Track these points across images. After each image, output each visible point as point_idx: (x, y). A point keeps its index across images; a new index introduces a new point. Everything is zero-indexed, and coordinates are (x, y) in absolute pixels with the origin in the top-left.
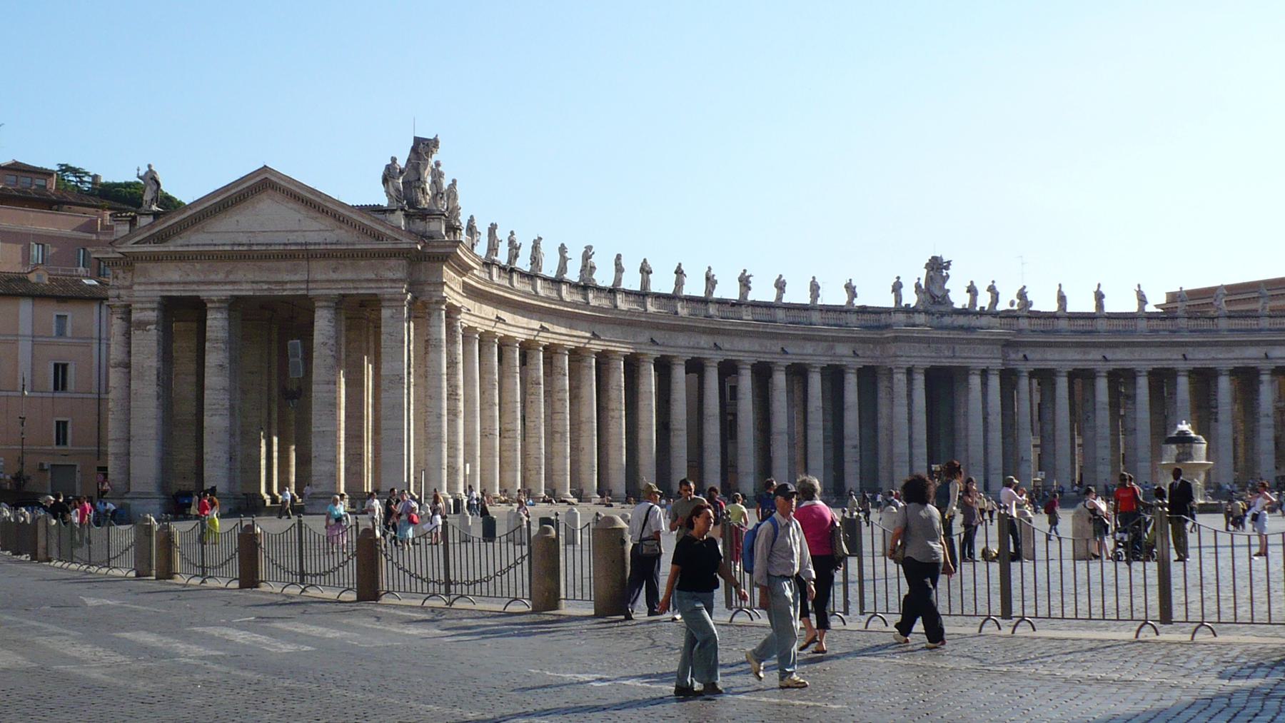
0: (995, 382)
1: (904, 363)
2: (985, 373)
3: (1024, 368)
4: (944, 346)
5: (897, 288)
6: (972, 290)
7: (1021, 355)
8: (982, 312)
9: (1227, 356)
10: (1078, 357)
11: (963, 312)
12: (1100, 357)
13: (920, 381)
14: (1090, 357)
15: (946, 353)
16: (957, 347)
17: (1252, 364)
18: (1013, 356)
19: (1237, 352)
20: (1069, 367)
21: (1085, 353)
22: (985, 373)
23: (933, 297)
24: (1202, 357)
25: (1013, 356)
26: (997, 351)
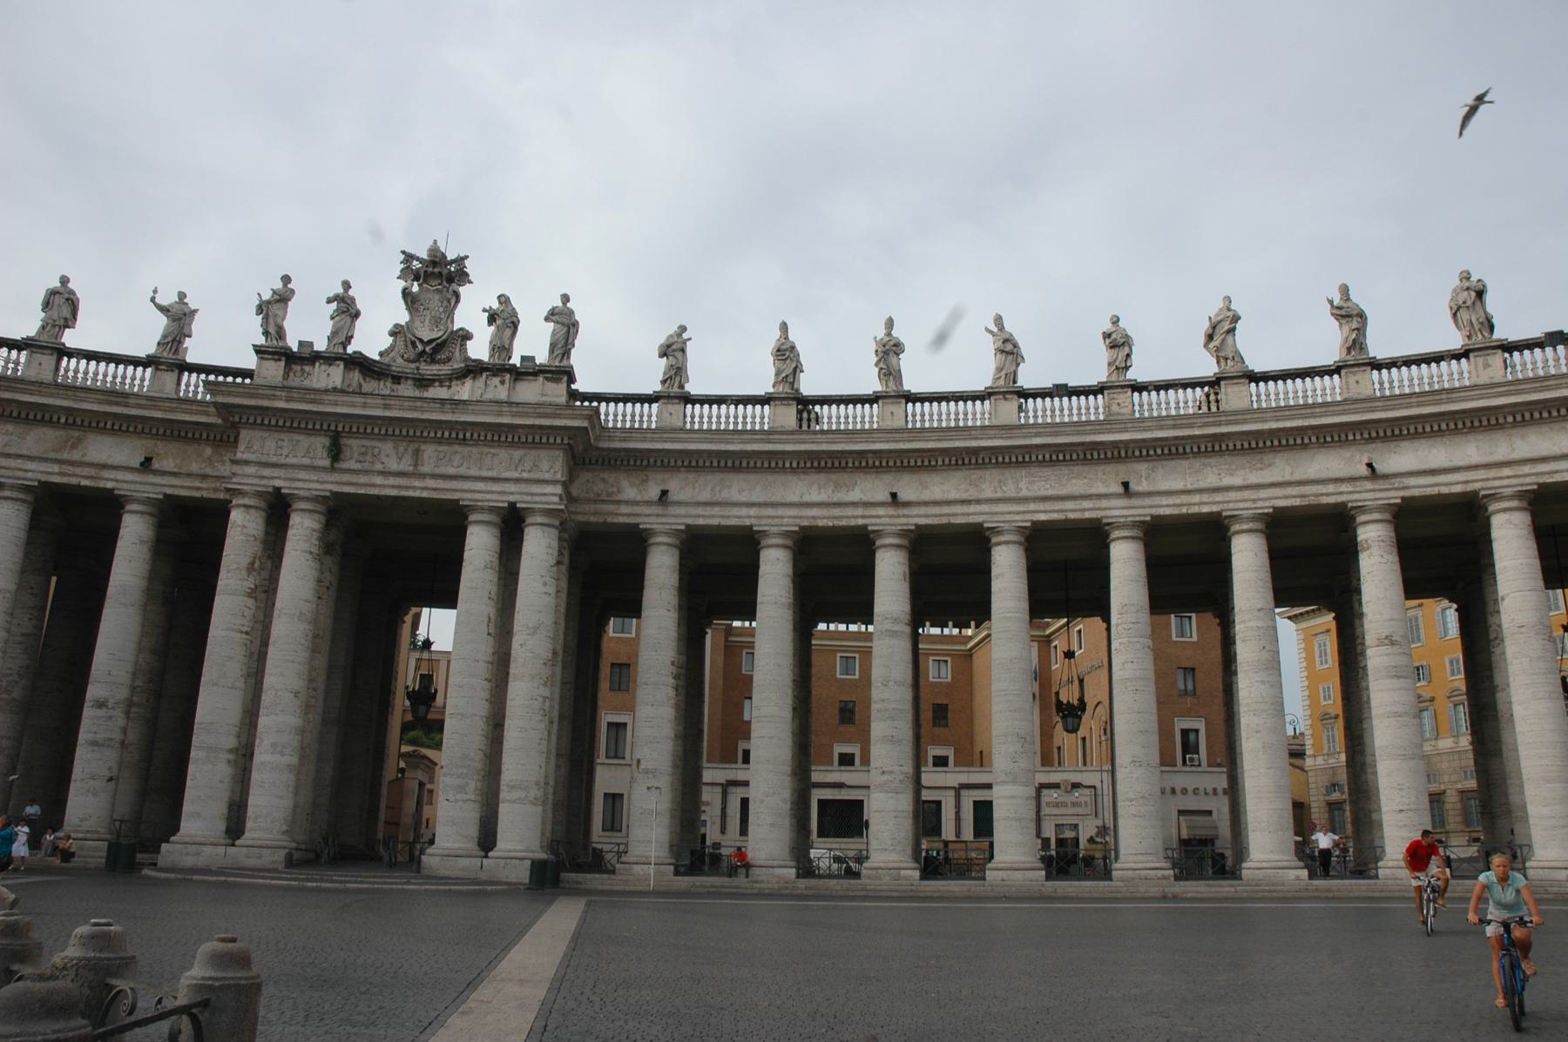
0: (539, 547)
1: (251, 479)
2: (511, 525)
3: (664, 524)
4: (387, 447)
5: (273, 307)
6: (504, 318)
7: (653, 493)
8: (529, 371)
9: (1254, 478)
10: (814, 496)
11: (475, 369)
12: (883, 496)
13: (303, 529)
14: (855, 495)
15: (393, 465)
16: (429, 451)
17: (1330, 496)
18: (630, 493)
19: (1281, 468)
20: (792, 520)
21: (838, 487)
22: (511, 525)
23: (413, 344)
24: (1178, 485)
25: (630, 493)
26: (552, 465)
